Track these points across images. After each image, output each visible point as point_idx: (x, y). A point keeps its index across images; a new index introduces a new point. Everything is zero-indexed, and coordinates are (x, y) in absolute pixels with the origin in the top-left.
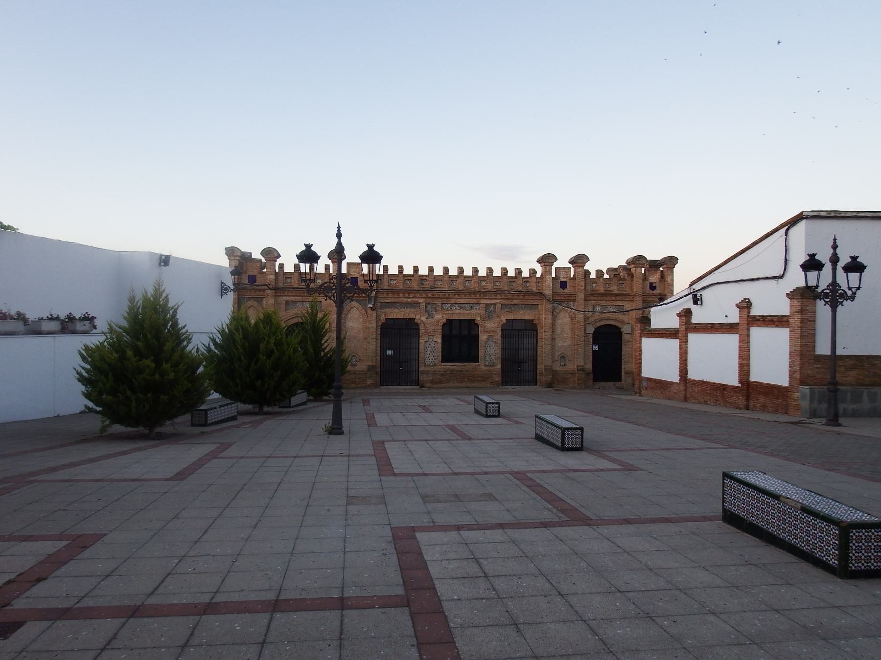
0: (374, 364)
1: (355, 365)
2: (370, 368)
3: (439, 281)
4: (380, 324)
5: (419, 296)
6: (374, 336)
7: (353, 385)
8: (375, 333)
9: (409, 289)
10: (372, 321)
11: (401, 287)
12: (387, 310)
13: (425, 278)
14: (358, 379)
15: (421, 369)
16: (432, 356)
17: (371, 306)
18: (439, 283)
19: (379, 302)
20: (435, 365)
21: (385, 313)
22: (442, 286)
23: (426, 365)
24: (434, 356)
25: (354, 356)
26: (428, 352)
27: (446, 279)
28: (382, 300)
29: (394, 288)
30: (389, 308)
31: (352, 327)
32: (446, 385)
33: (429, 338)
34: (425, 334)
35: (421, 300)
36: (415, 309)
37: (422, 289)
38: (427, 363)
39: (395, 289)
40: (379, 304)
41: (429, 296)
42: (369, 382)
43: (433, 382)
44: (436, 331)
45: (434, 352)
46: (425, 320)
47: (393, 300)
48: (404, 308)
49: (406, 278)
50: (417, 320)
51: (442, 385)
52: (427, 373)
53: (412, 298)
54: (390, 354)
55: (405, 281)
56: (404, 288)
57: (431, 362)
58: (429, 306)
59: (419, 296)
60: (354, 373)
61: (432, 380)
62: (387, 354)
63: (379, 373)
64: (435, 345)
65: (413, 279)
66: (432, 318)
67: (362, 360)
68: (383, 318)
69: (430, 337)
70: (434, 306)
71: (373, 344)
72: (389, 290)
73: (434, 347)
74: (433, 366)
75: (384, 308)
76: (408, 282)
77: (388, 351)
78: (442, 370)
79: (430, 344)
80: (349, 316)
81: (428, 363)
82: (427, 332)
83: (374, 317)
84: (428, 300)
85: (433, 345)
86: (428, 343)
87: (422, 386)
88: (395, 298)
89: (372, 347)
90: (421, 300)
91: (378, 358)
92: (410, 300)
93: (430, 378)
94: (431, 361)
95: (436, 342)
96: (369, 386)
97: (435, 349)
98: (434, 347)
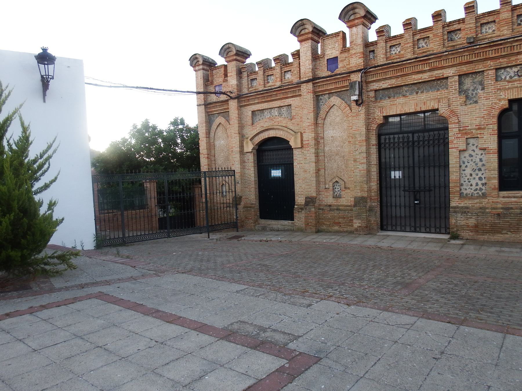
0: (365, 195)
1: (340, 197)
2: (359, 201)
3: (489, 26)
4: (374, 126)
5: (444, 64)
6: (364, 149)
7: (336, 228)
8: (365, 144)
9: (424, 54)
10: (360, 123)
11: (409, 56)
12: (386, 102)
13: (456, 27)
14: (341, 218)
15: (453, 204)
16: (477, 177)
17: (355, 98)
18: (489, 31)
19: (371, 91)
20: (484, 196)
21: (382, 107)
22: (497, 33)
23: (462, 196)
24: (480, 179)
25: (337, 182)
26: (468, 171)
27: (506, 15)
28: (375, 86)
29: (395, 61)
30: (389, 98)
31: (332, 137)
32: (508, 236)
33: (468, 144)
34: (459, 135)
35: (448, 72)
36: (438, 90)
37: (449, 49)
38: (465, 192)
39: (398, 60)
40: (372, 94)
41: (465, 59)
42: (357, 223)
43: (476, 228)
44: (484, 129)
45: (480, 170)
46: (461, 110)
47: (394, 82)
48: (417, 93)
49: (418, 37)
50: (443, 111)
51: (498, 237)
52: (465, 211)
53: (430, 70)
54: (397, 177)
55: (415, 43)
56: (413, 57)
57: (476, 190)
58: (468, 82)
59: (444, 64)
60: (337, 209)
61: (476, 226)
62: (393, 177)
63: (378, 209)
64: (484, 158)
65: (431, 36)
66: (476, 102)
67: (349, 188)
68: (378, 116)
69: (472, 141)
70: (479, 78)
71: (362, 161)
72: (385, 65)
73: (481, 160)
74: (479, 197)
75: (381, 99)
76: (422, 43)
77: (393, 173)
78: (500, 206)
79: (471, 156)
80: (328, 120)
81: (468, 191)
82: (463, 132)
83: (362, 116)
84: (465, 69)
85: (479, 157)
86: (466, 154)
87: (455, 237)
88: (397, 77)
89: (361, 167)
90: (448, 72)
91: (374, 185)
92: (426, 76)
93: (472, 221)
94: (474, 187)
95: (484, 149)
96: (356, 230)
97: (483, 165)
98: (481, 160)
